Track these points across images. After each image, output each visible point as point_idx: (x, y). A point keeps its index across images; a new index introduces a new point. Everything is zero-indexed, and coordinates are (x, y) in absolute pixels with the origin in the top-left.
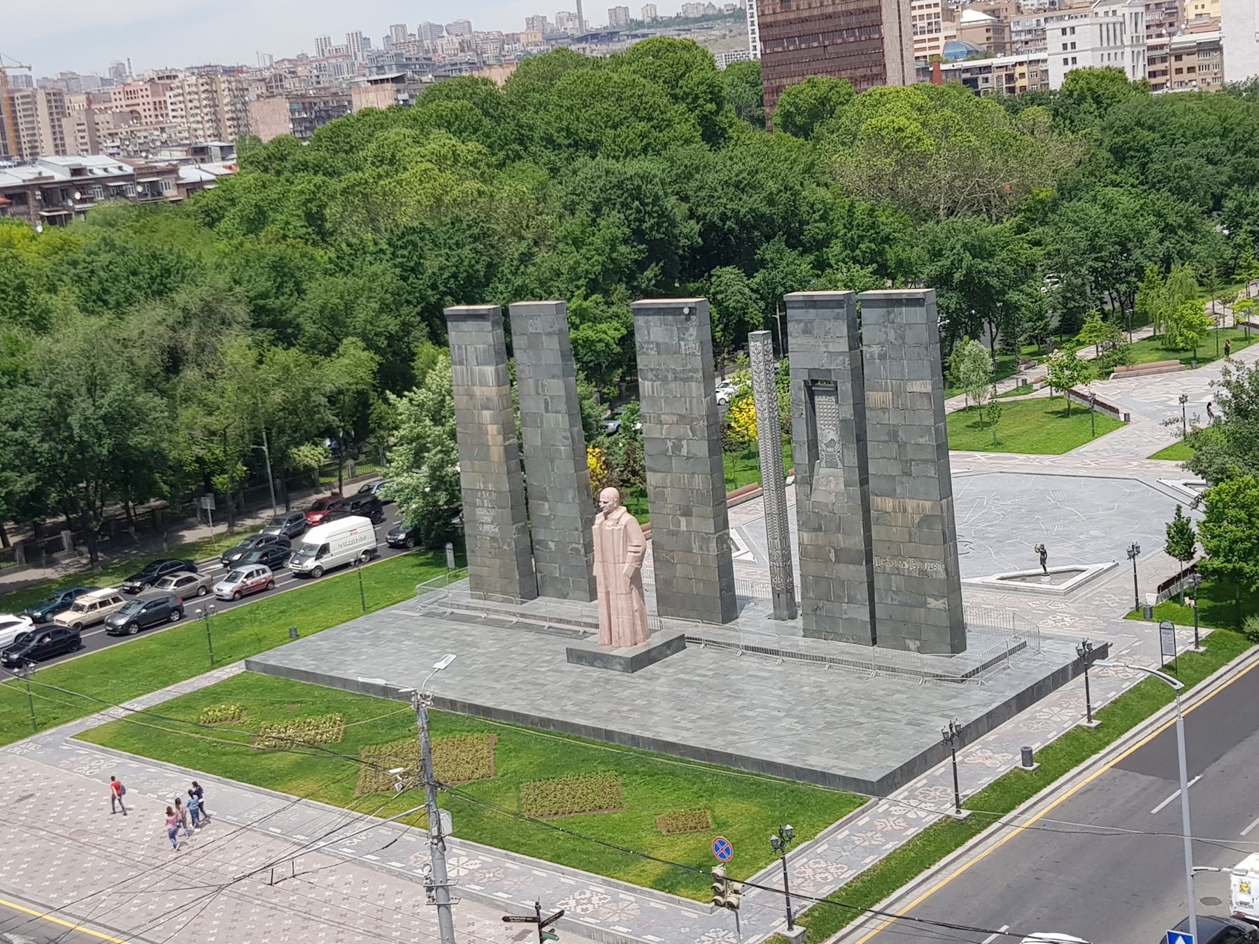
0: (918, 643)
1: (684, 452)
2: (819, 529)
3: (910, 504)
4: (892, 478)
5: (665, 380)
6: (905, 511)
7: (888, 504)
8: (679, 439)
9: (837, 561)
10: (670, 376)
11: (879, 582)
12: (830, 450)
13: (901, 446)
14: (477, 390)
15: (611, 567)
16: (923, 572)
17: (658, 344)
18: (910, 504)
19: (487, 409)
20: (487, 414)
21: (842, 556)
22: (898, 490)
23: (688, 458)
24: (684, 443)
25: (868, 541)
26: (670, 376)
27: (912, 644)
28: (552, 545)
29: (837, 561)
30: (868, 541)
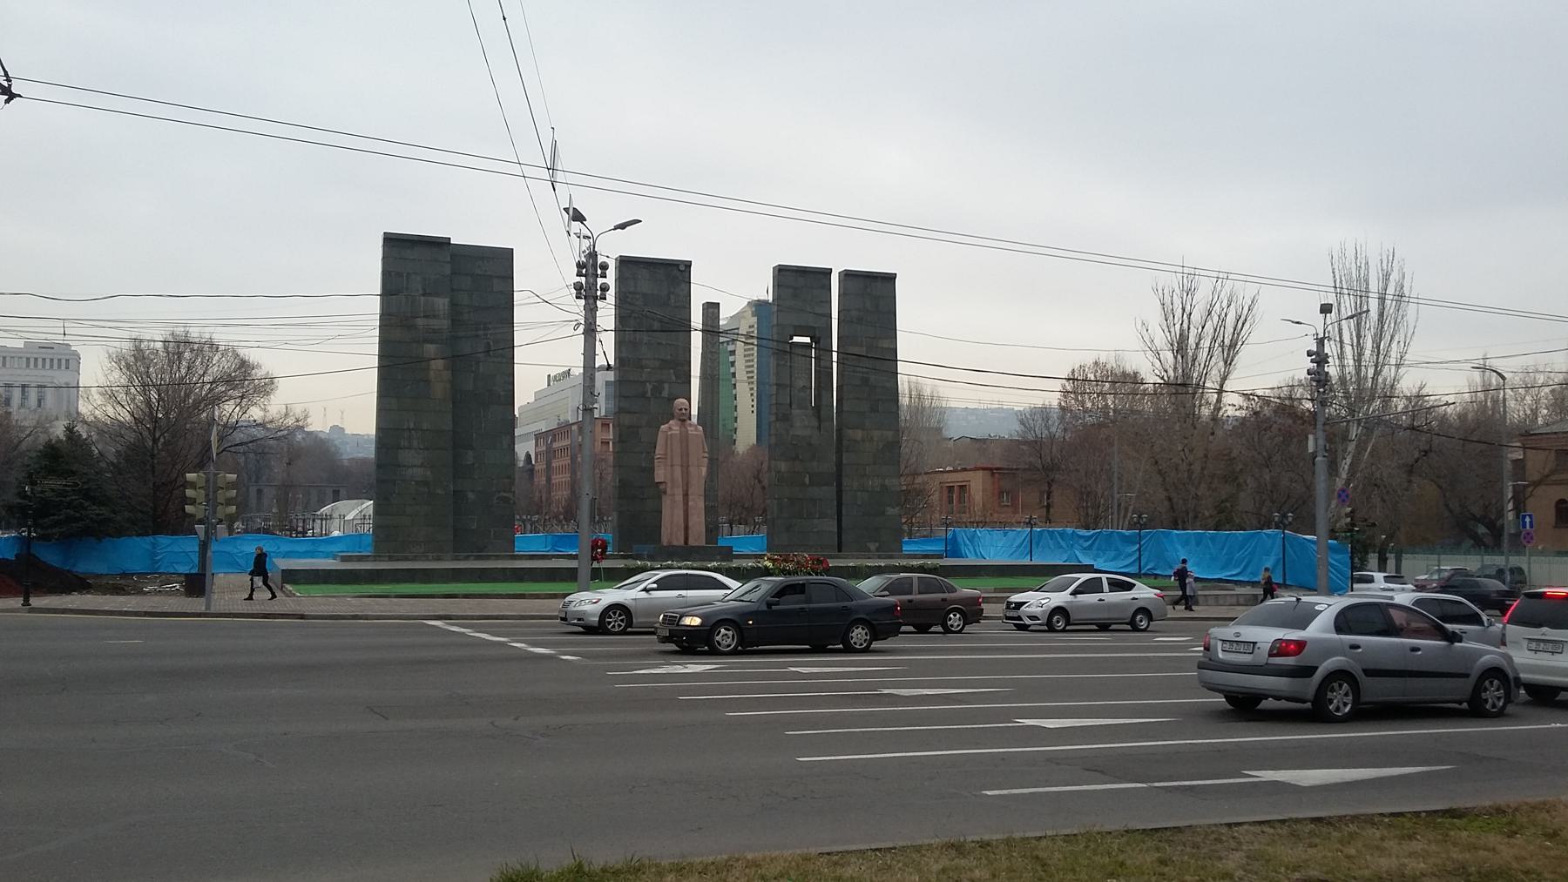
1: (665, 394)
2: (797, 458)
3: (876, 434)
6: (872, 439)
7: (859, 434)
8: (662, 382)
9: (811, 484)
11: (846, 498)
14: (420, 322)
16: (883, 486)
17: (644, 295)
19: (431, 342)
20: (431, 349)
24: (666, 386)
25: (839, 464)
27: (873, 546)
28: (471, 496)
29: (811, 484)
30: (839, 464)
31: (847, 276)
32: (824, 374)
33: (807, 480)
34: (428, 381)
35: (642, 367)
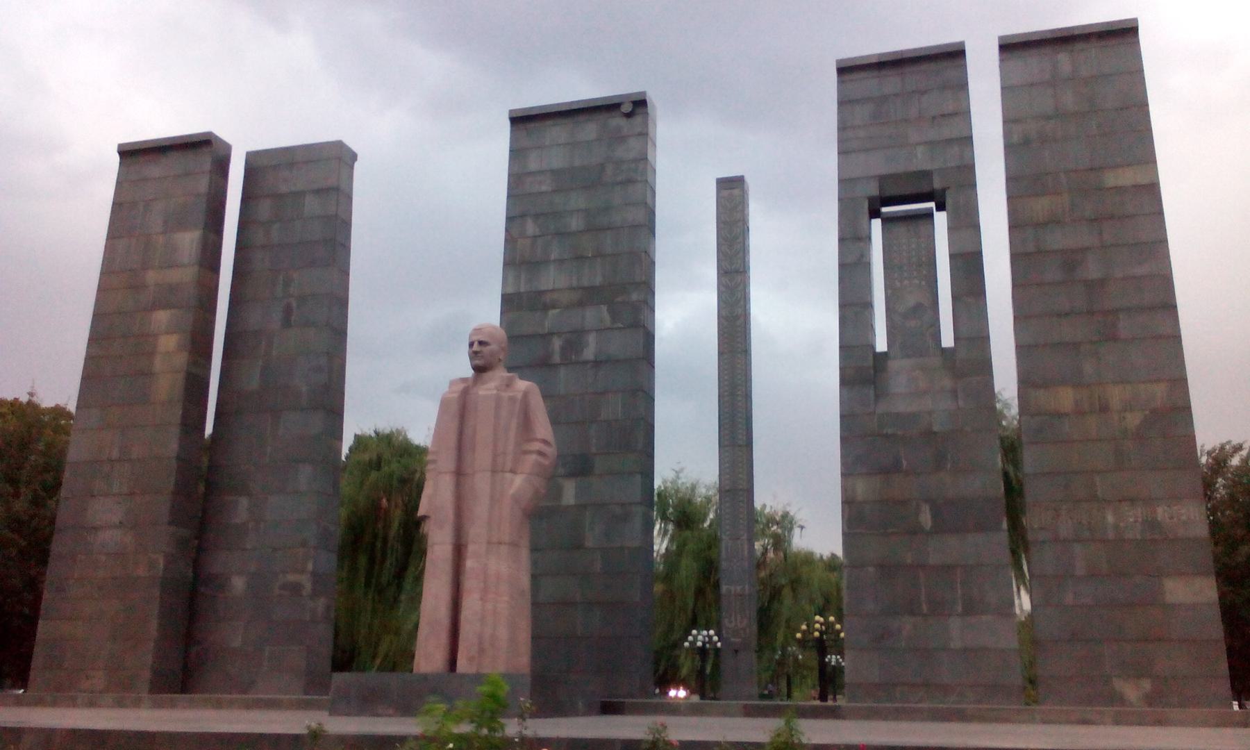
0: (1146, 685)
1: (589, 353)
4: (1075, 346)
5: (561, 234)
6: (1104, 409)
7: (1066, 398)
10: (575, 223)
12: (912, 323)
13: (1095, 287)
14: (152, 277)
15: (481, 483)
16: (1152, 524)
18: (1116, 395)
20: (162, 317)
21: (953, 517)
22: (1088, 368)
23: (597, 363)
24: (592, 339)
26: (575, 223)
27: (1132, 691)
28: (238, 584)
29: (940, 527)
31: (1010, 47)
32: (969, 266)
33: (926, 518)
34: (148, 374)
35: (546, 308)
